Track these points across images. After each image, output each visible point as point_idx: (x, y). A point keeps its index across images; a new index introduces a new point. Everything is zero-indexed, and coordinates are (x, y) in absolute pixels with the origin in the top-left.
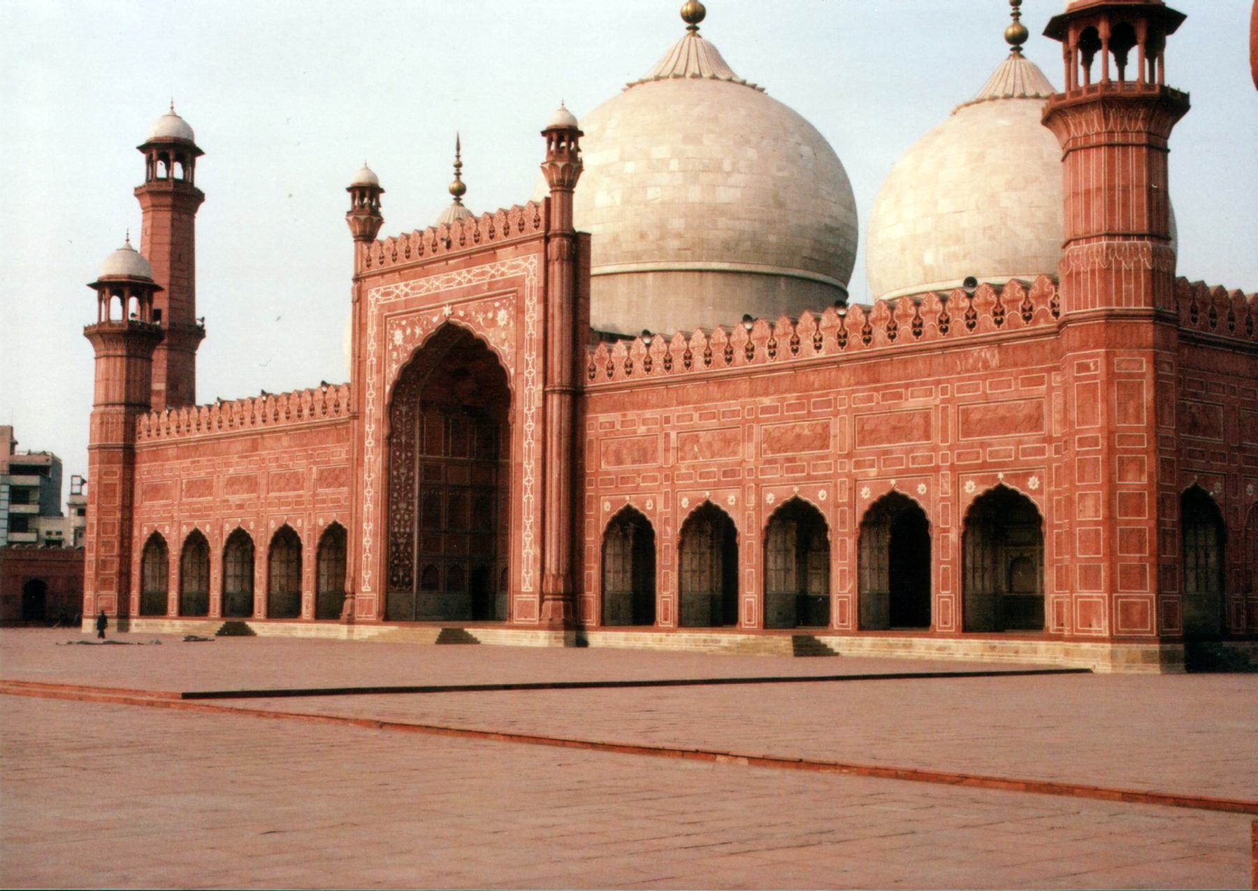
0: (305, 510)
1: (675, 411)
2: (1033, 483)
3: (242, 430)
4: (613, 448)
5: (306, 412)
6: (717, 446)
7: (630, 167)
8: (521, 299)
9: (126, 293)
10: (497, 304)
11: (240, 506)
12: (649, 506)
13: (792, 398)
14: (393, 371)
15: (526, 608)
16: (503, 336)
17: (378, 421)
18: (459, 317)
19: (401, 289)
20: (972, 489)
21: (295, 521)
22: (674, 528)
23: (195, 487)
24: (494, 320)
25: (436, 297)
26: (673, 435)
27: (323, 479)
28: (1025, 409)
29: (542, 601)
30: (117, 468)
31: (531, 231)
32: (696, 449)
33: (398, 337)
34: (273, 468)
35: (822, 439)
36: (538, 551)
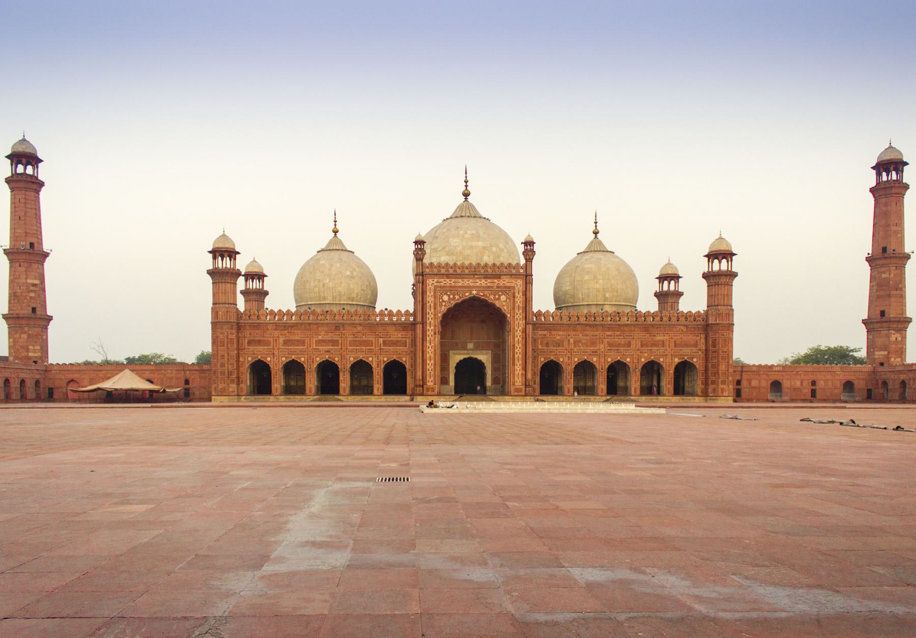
2: (695, 360)
4: (545, 341)
7: (494, 249)
8: (514, 293)
9: (226, 254)
12: (561, 360)
13: (618, 333)
14: (444, 309)
15: (517, 390)
17: (435, 326)
20: (677, 360)
21: (368, 358)
24: (499, 299)
25: (469, 287)
26: (572, 340)
27: (385, 343)
28: (693, 342)
30: (234, 331)
33: (446, 298)
34: (351, 338)
35: (629, 345)
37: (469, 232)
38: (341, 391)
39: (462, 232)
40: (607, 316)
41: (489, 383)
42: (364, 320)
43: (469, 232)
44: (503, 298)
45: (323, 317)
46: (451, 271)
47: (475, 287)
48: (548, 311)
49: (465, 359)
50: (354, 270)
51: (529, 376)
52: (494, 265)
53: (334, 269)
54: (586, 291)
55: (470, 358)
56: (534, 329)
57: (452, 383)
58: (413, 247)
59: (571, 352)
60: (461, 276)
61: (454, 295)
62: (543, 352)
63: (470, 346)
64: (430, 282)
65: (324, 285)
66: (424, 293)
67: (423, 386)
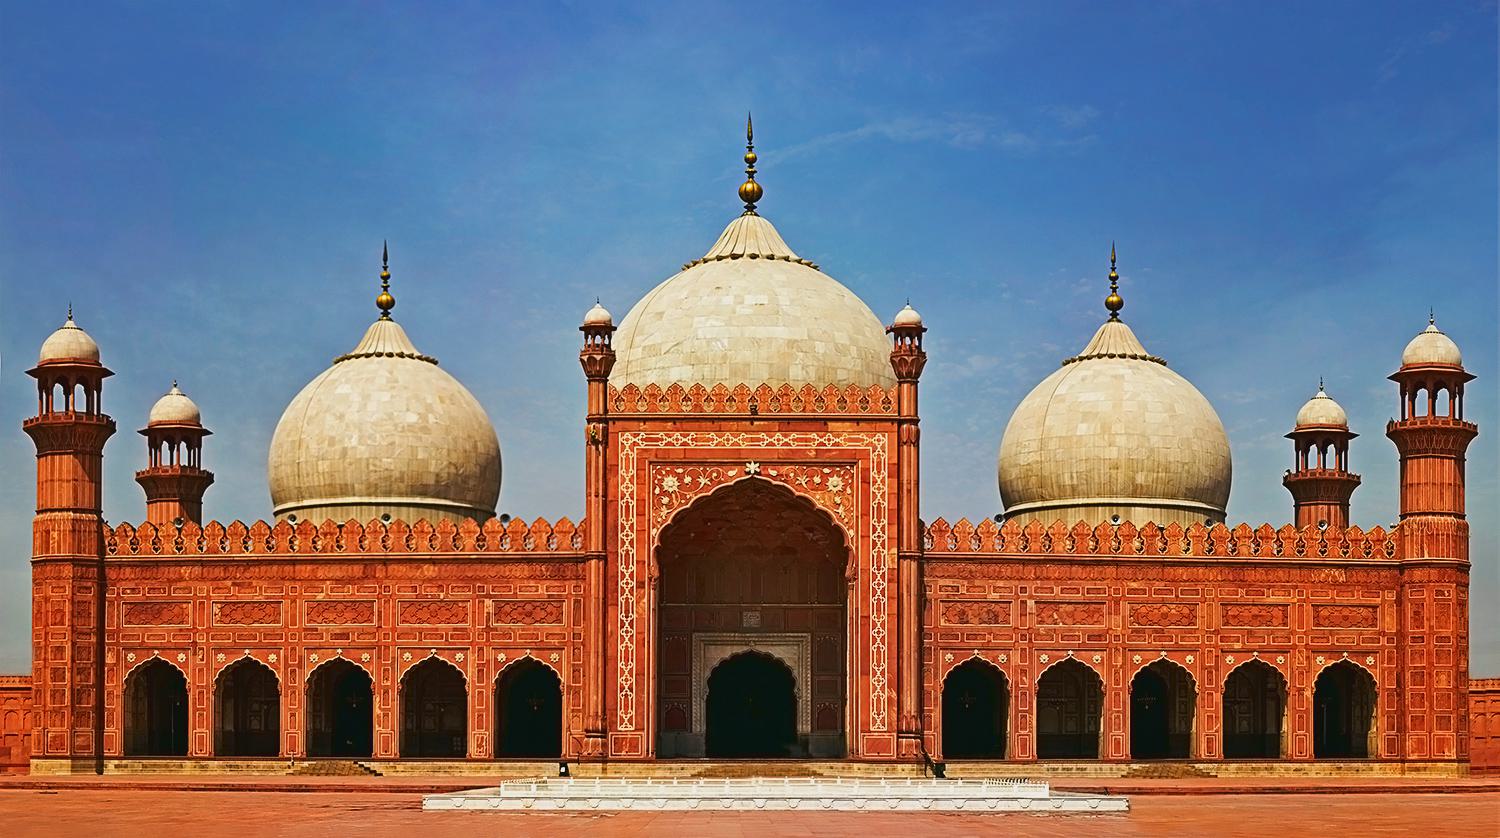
0: (471, 643)
1: (1031, 586)
3: (337, 554)
5: (470, 541)
6: (1079, 615)
7: (820, 347)
8: (866, 471)
10: (826, 471)
11: (344, 635)
12: (1002, 657)
14: (666, 516)
15: (877, 745)
16: (838, 500)
18: (769, 476)
19: (676, 440)
22: (1031, 679)
23: (230, 609)
24: (823, 486)
26: (1031, 603)
27: (499, 612)
29: (898, 737)
31: (876, 410)
32: (1056, 617)
33: (670, 483)
36: (894, 695)
37: (749, 300)
38: (378, 748)
39: (728, 300)
40: (1129, 538)
41: (804, 727)
42: (444, 547)
43: (749, 300)
44: (835, 482)
45: (330, 541)
46: (687, 409)
47: (754, 452)
48: (963, 523)
49: (735, 657)
50: (429, 409)
51: (910, 704)
52: (808, 389)
53: (372, 407)
54: (1083, 467)
55: (751, 655)
56: (921, 573)
57: (699, 726)
58: (580, 341)
59: (1028, 635)
60: (717, 422)
61: (695, 476)
62: (949, 634)
63: (752, 619)
64: (626, 439)
65: (344, 452)
66: (609, 470)
67: (604, 733)
